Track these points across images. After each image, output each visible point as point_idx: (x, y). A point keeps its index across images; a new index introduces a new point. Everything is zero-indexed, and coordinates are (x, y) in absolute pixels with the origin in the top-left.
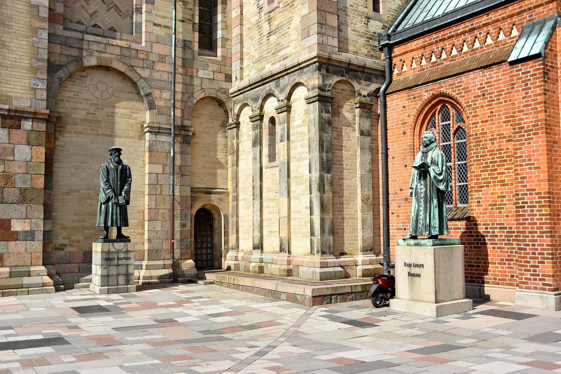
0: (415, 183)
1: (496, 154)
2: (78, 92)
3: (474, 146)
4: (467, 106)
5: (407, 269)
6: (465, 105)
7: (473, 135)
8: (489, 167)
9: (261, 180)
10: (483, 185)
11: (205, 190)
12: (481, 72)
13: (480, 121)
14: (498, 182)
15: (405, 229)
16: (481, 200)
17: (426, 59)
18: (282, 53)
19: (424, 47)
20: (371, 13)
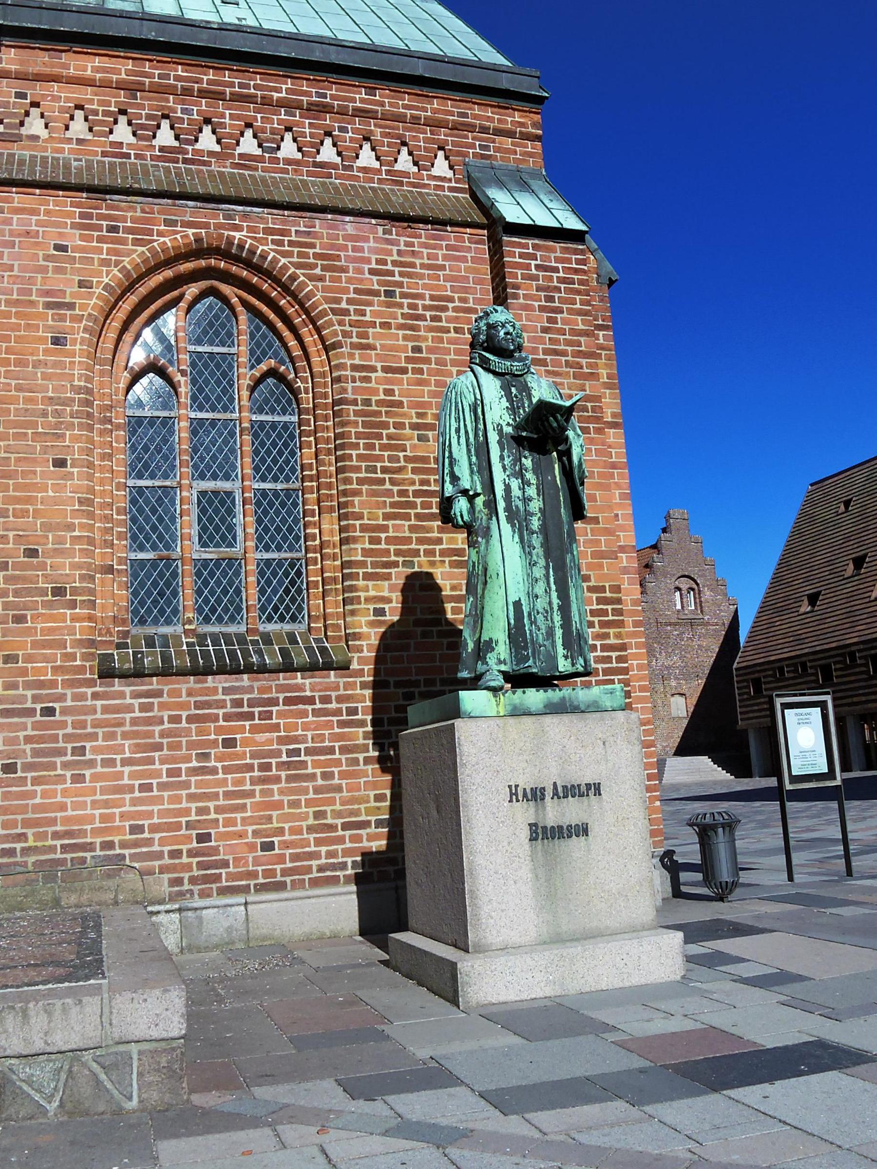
0: (499, 476)
3: (358, 435)
4: (334, 312)
5: (525, 813)
6: (326, 306)
7: (355, 402)
8: (413, 505)
10: (393, 558)
12: (380, 229)
13: (379, 366)
14: (443, 553)
15: (49, 712)
16: (387, 607)
19: (132, 89)
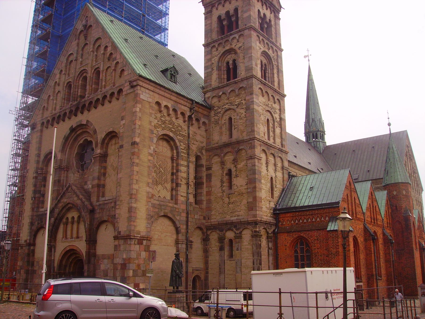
1: (322, 261)
2: (156, 227)
3: (314, 257)
9: (224, 266)
11: (196, 269)
17: (294, 221)
18: (236, 213)
19: (293, 217)
20: (270, 199)
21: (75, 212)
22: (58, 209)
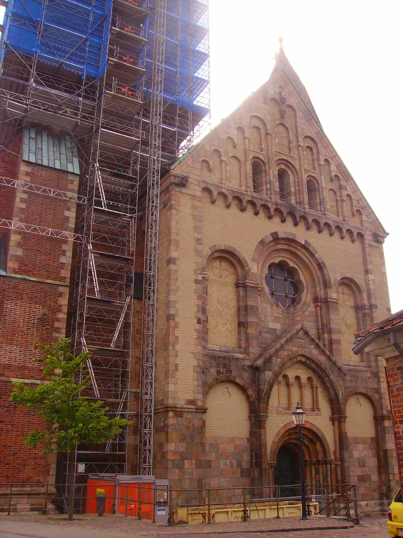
21: (301, 371)
22: (279, 360)
